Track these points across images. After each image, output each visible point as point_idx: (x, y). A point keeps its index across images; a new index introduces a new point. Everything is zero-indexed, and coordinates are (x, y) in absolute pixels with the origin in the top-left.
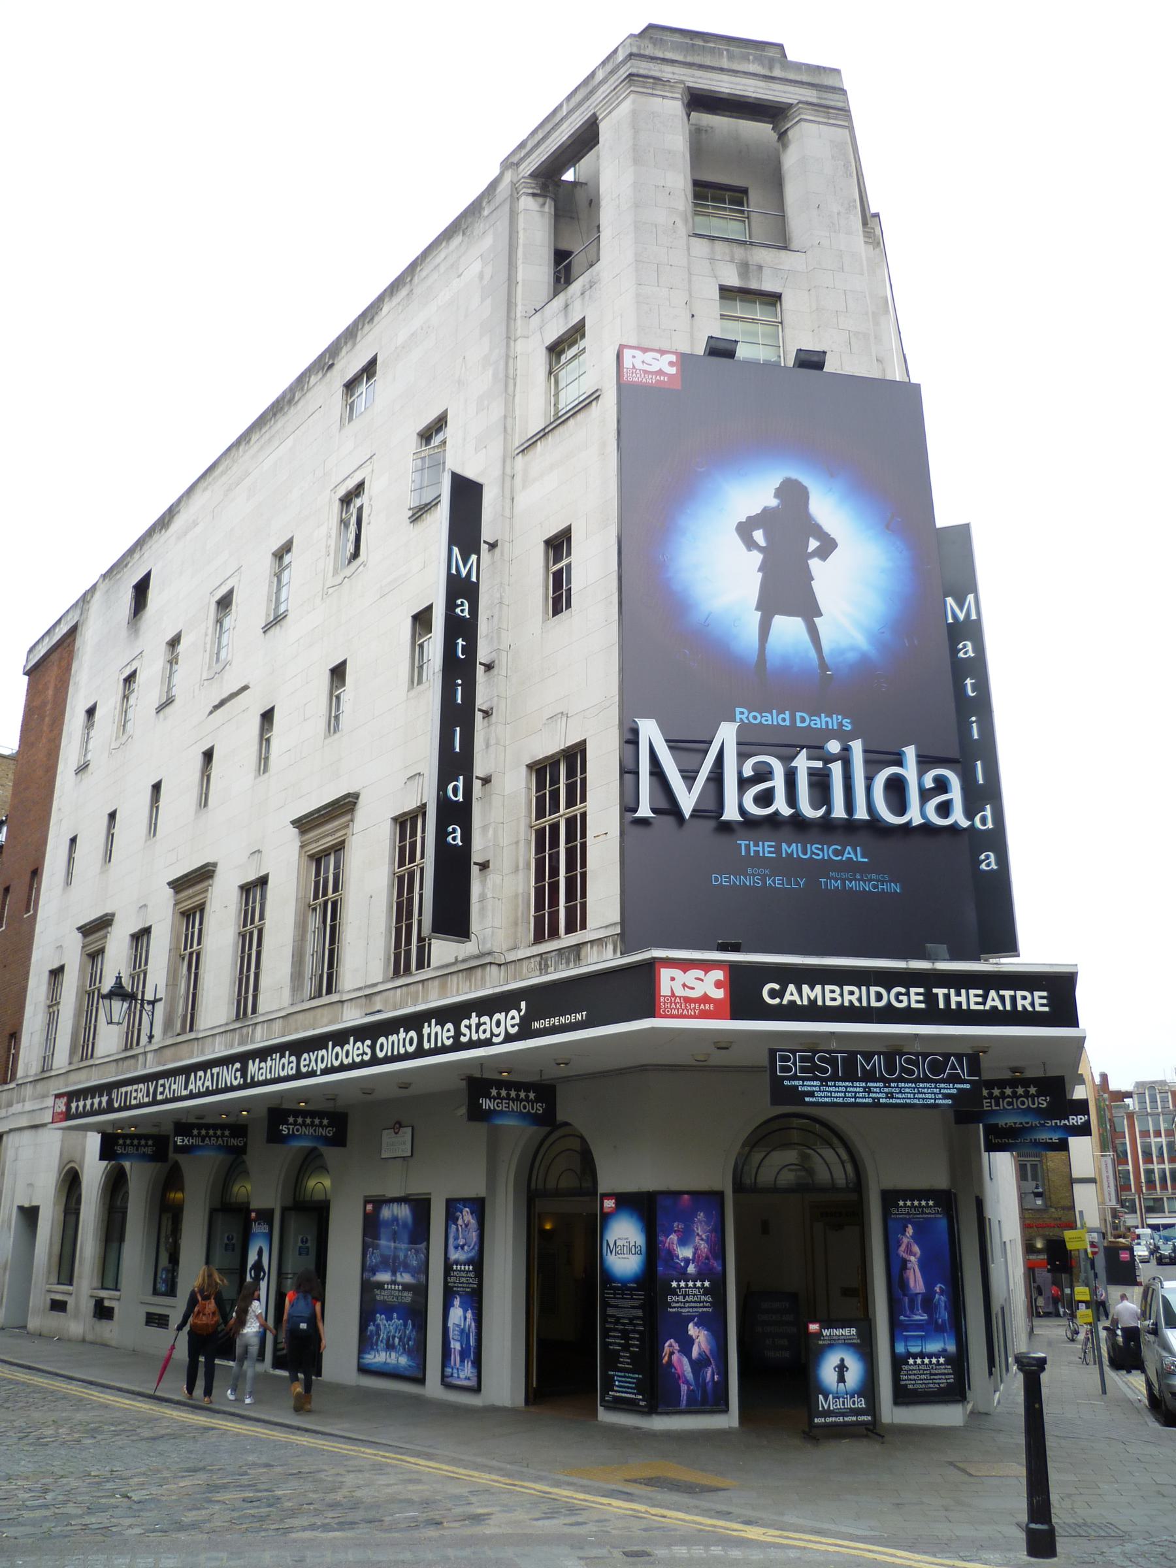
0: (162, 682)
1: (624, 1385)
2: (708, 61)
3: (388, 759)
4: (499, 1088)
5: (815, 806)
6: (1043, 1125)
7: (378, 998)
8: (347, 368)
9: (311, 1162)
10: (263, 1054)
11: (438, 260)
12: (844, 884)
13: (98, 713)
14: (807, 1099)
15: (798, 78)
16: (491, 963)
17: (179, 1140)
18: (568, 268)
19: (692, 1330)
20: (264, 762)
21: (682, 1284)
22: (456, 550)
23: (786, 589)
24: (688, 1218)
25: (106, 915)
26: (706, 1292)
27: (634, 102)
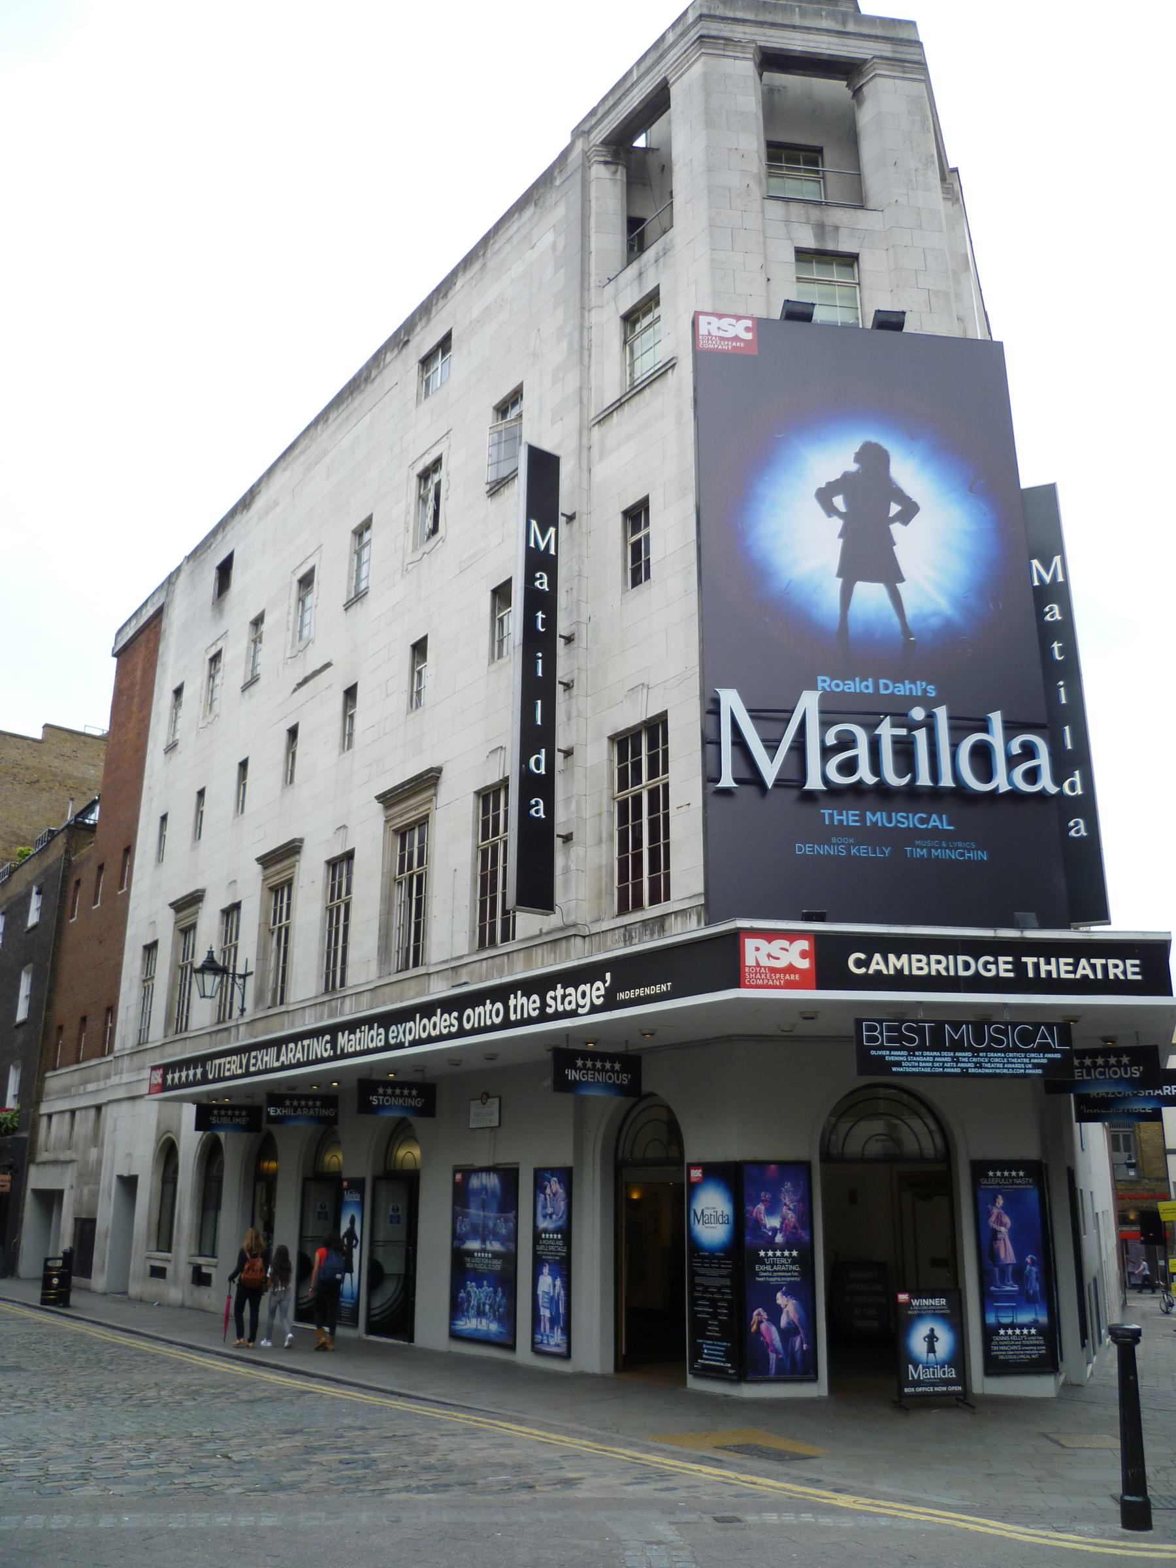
0: (247, 662)
1: (713, 1353)
3: (470, 732)
4: (584, 1059)
5: (900, 775)
6: (1136, 1095)
7: (464, 971)
8: (423, 344)
9: (400, 1132)
10: (352, 1026)
11: (510, 232)
12: (929, 853)
13: (186, 693)
14: (894, 1069)
15: (873, 32)
16: (575, 935)
17: (272, 1111)
18: (641, 236)
19: (780, 1299)
20: (347, 739)
21: (770, 1253)
22: (534, 523)
23: (869, 554)
24: (775, 1188)
25: (197, 891)
26: (794, 1261)
27: (705, 64)
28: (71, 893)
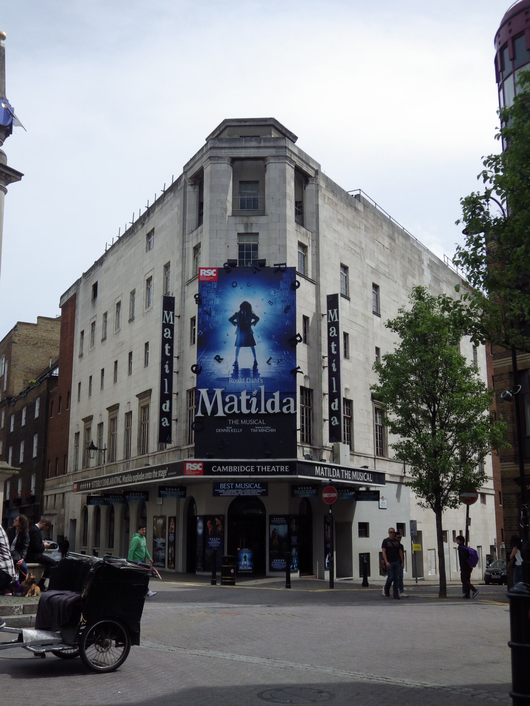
0: (103, 330)
2: (238, 145)
26: (219, 541)
28: (50, 407)
